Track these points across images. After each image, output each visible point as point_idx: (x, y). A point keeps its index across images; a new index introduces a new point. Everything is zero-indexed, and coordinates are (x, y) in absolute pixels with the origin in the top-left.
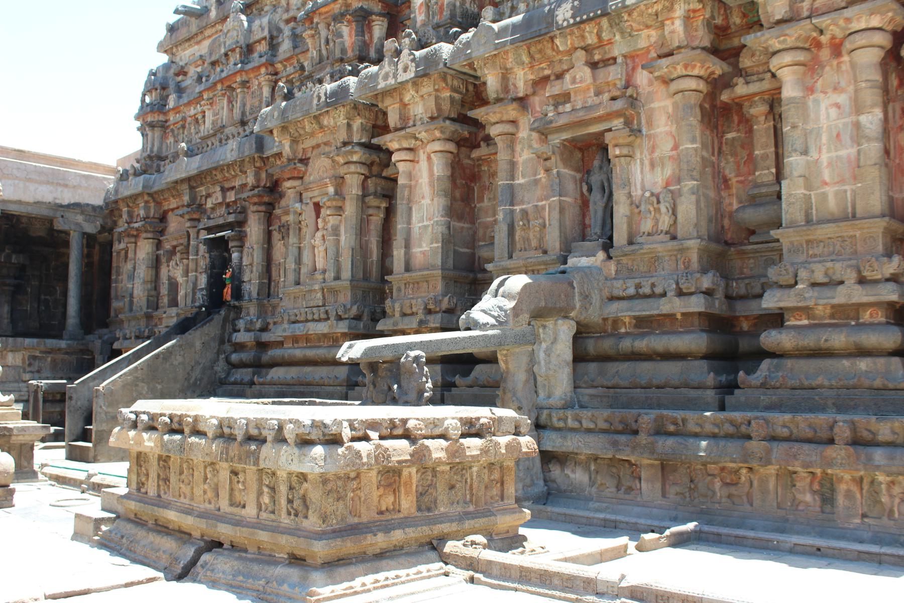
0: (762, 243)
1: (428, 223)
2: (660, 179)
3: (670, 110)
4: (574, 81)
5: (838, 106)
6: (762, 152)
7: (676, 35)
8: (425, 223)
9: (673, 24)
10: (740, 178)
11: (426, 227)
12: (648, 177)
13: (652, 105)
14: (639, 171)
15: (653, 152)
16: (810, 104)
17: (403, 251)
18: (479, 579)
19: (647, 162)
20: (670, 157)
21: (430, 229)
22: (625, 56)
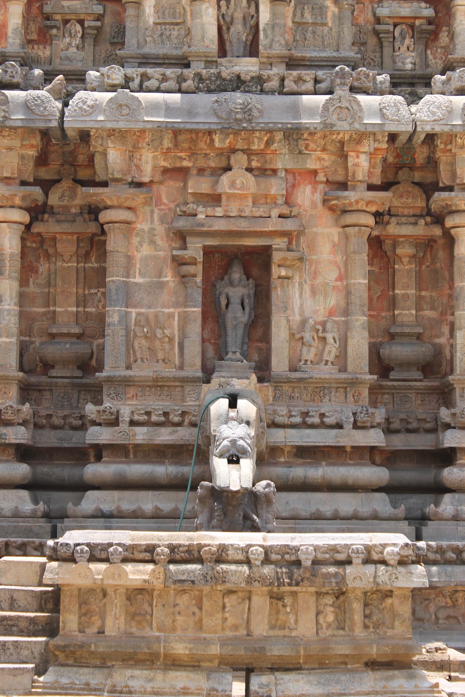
0: (404, 380)
2: (322, 308)
3: (336, 239)
4: (233, 184)
6: (403, 292)
7: (361, 169)
9: (358, 157)
10: (372, 313)
12: (309, 303)
13: (314, 229)
14: (297, 295)
15: (315, 278)
18: (457, 677)
19: (307, 288)
20: (334, 287)
22: (286, 170)
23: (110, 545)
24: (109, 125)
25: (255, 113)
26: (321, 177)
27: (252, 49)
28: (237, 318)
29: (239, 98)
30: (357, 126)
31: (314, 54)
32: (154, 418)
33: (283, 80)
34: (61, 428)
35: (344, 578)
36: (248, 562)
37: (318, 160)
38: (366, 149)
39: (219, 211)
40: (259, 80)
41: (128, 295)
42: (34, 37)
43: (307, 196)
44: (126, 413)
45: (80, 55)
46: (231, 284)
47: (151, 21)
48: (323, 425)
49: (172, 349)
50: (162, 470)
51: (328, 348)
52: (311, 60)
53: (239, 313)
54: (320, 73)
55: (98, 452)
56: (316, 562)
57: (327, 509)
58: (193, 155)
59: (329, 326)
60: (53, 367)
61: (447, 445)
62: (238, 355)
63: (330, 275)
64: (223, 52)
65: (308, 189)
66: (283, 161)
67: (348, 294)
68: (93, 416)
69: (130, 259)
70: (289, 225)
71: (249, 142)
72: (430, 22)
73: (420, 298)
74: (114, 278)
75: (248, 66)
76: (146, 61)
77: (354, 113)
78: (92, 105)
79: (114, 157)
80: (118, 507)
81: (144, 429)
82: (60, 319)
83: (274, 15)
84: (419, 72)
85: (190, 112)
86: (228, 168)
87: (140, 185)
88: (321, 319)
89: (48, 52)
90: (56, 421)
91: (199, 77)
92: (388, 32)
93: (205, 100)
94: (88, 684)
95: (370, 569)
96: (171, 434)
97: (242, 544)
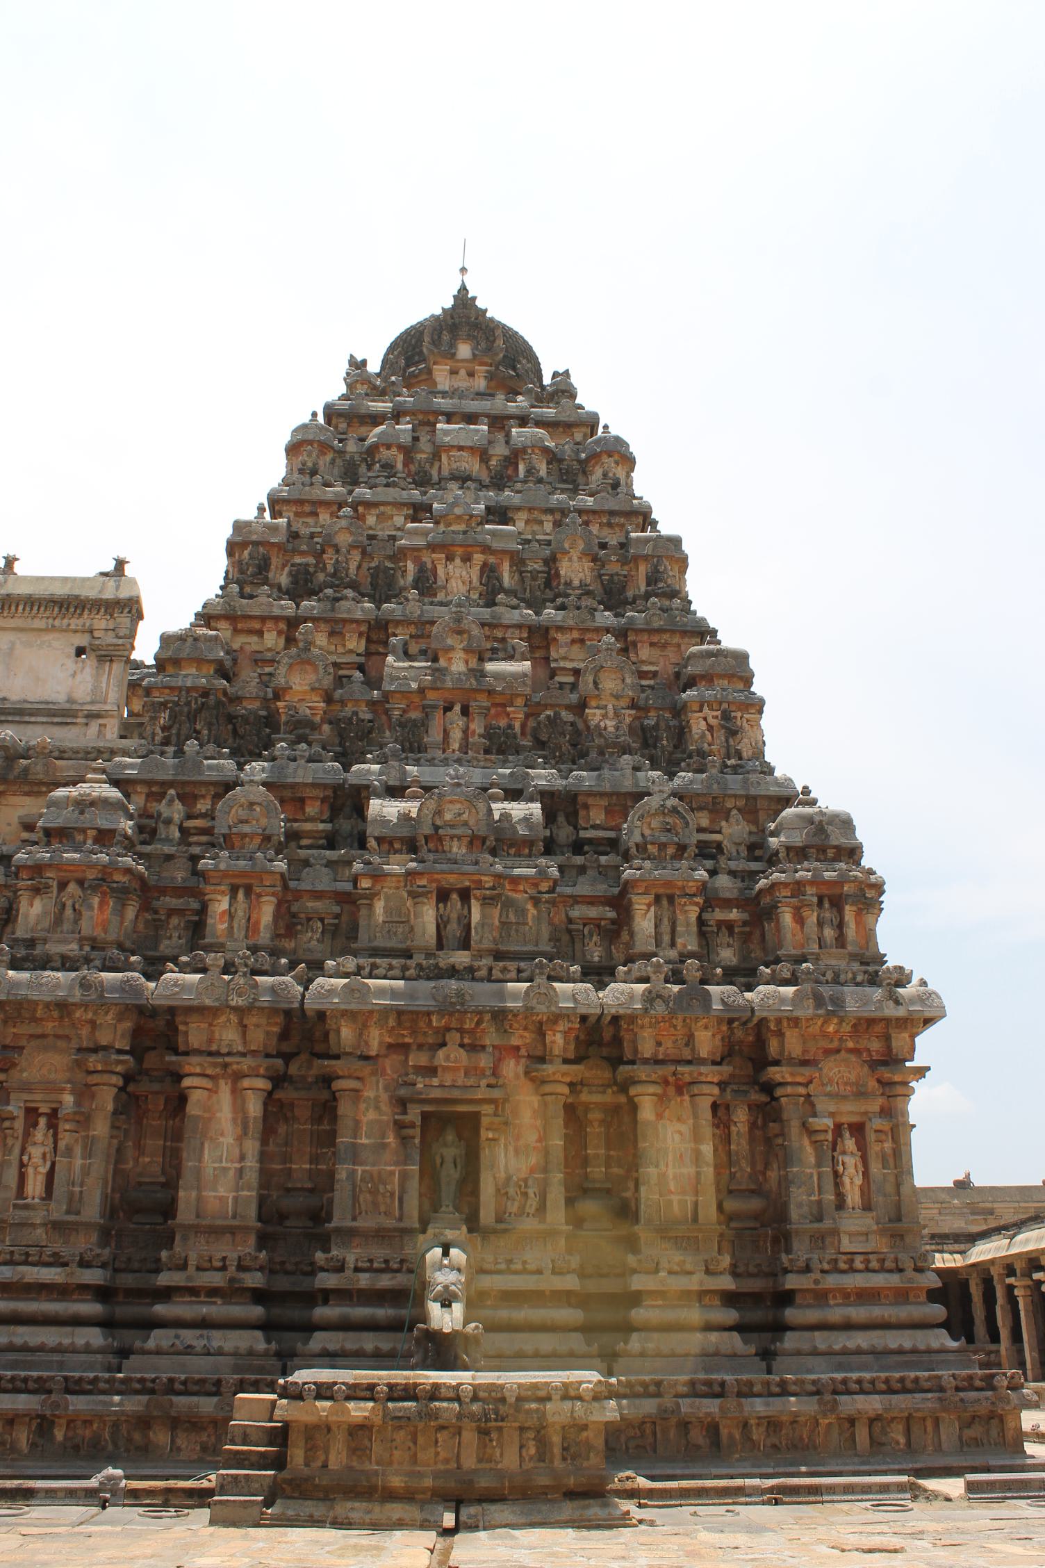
1: (229, 1165)
3: (536, 1105)
4: (447, 1058)
5: (680, 1133)
8: (224, 1164)
11: (225, 1169)
16: (660, 1127)
17: (194, 1194)
19: (511, 1149)
21: (231, 1173)
22: (494, 1046)
23: (335, 1383)
24: (343, 1007)
25: (468, 998)
26: (523, 1052)
27: (465, 944)
28: (450, 1175)
29: (453, 984)
30: (553, 1009)
31: (517, 948)
32: (376, 1265)
33: (490, 969)
34: (293, 1273)
35: (544, 1413)
36: (458, 1399)
37: (520, 1037)
38: (561, 1028)
39: (435, 1081)
40: (471, 970)
41: (355, 1154)
42: (282, 931)
44: (351, 1260)
45: (321, 947)
46: (445, 1145)
47: (381, 920)
48: (524, 1271)
49: (393, 1201)
50: (382, 1313)
51: (529, 1202)
52: (515, 953)
53: (452, 1171)
54: (522, 964)
55: (326, 1296)
56: (519, 1399)
57: (529, 1348)
58: (414, 1032)
59: (530, 1182)
60: (287, 1218)
61: (634, 1288)
62: (451, 1208)
63: (531, 1138)
64: (440, 945)
65: (512, 1062)
67: (546, 1153)
68: (322, 1263)
69: (357, 1123)
70: (496, 1094)
71: (462, 1021)
72: (613, 922)
73: (608, 1157)
74: (343, 1140)
75: (461, 958)
76: (375, 952)
77: (551, 997)
79: (347, 1033)
80: (342, 1347)
81: (367, 1275)
83: (483, 916)
84: (605, 963)
85: (411, 996)
86: (444, 1044)
87: (366, 1058)
88: (523, 1176)
89: (293, 945)
90: (289, 1267)
91: (420, 966)
92: (578, 930)
93: (426, 986)
94: (311, 1516)
95: (567, 1405)
96: (391, 1279)
97: (454, 1383)
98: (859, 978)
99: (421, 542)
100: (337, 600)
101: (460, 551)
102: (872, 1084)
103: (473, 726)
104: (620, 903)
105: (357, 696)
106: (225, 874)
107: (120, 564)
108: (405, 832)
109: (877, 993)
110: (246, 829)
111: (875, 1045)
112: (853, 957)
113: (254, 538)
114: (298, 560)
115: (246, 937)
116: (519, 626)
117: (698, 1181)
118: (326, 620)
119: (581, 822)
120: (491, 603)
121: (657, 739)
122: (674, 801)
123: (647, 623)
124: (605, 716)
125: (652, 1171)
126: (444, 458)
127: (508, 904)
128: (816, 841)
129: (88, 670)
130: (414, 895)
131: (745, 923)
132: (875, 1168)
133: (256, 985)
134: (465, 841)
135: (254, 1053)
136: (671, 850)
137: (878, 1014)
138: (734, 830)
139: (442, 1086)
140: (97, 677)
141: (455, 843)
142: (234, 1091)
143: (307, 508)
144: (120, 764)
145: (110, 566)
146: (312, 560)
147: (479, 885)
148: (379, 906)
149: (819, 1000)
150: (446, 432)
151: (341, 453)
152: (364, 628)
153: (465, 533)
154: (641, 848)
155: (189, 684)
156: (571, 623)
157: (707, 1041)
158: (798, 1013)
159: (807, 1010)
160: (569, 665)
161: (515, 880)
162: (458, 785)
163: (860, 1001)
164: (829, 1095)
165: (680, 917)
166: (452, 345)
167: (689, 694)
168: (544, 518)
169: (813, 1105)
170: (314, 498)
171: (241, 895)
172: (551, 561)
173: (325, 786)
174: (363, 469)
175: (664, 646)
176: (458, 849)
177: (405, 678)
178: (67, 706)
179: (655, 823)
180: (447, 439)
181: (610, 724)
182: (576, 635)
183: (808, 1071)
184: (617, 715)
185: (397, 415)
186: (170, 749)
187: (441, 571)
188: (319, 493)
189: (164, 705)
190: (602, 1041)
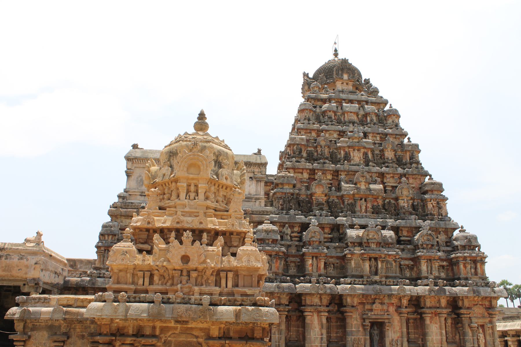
12: (393, 335)
26: (395, 305)
29: (378, 287)
37: (394, 301)
39: (373, 313)
40: (381, 282)
43: (392, 309)
45: (333, 272)
46: (374, 330)
58: (366, 299)
63: (397, 328)
66: (386, 301)
67: (402, 333)
69: (352, 324)
70: (389, 317)
71: (380, 297)
72: (412, 265)
75: (377, 278)
77: (404, 290)
78: (343, 288)
79: (349, 300)
82: (332, 338)
83: (382, 266)
85: (368, 290)
87: (353, 306)
88: (396, 339)
98: (483, 285)
99: (345, 145)
100: (324, 163)
101: (357, 148)
102: (486, 314)
103: (368, 205)
104: (416, 260)
105: (333, 194)
106: (311, 253)
107: (259, 151)
108: (358, 241)
109: (489, 289)
110: (314, 239)
111: (487, 303)
112: (480, 278)
113: (297, 143)
114: (309, 149)
115: (317, 271)
116: (376, 173)
117: (442, 341)
118: (321, 170)
119: (400, 235)
120: (367, 165)
121: (418, 209)
122: (430, 232)
123: (412, 172)
124: (404, 202)
125: (430, 338)
126: (346, 115)
127: (387, 262)
128: (469, 244)
129: (254, 184)
130: (363, 260)
131: (447, 266)
132: (488, 338)
133: (325, 287)
134: (375, 244)
135: (323, 306)
136: (430, 246)
137: (490, 296)
138: (442, 238)
139: (375, 314)
140: (257, 186)
141: (373, 244)
142: (318, 316)
143: (308, 131)
144: (272, 217)
145: (256, 151)
146: (313, 149)
147: (381, 257)
148: (353, 262)
149: (474, 292)
150: (347, 107)
151: (315, 112)
152: (332, 172)
153: (358, 142)
154: (422, 245)
155: (288, 192)
156: (391, 172)
157: (444, 302)
158: (469, 295)
159: (471, 294)
160: (391, 185)
161: (389, 255)
162: (373, 227)
163: (485, 292)
164: (475, 317)
165: (433, 266)
166: (342, 75)
167: (426, 196)
168: (377, 135)
169: (471, 320)
170: (311, 128)
171: (314, 259)
172: (382, 151)
173: (330, 224)
174: (321, 117)
175: (416, 179)
176: (373, 246)
177: (348, 190)
178: (249, 196)
179: (425, 238)
180: (347, 109)
181: (406, 205)
182: (392, 175)
183: (470, 311)
184: (407, 202)
185: (330, 100)
186: (285, 212)
187: (351, 154)
188: (311, 127)
189: (281, 197)
190: (416, 302)
